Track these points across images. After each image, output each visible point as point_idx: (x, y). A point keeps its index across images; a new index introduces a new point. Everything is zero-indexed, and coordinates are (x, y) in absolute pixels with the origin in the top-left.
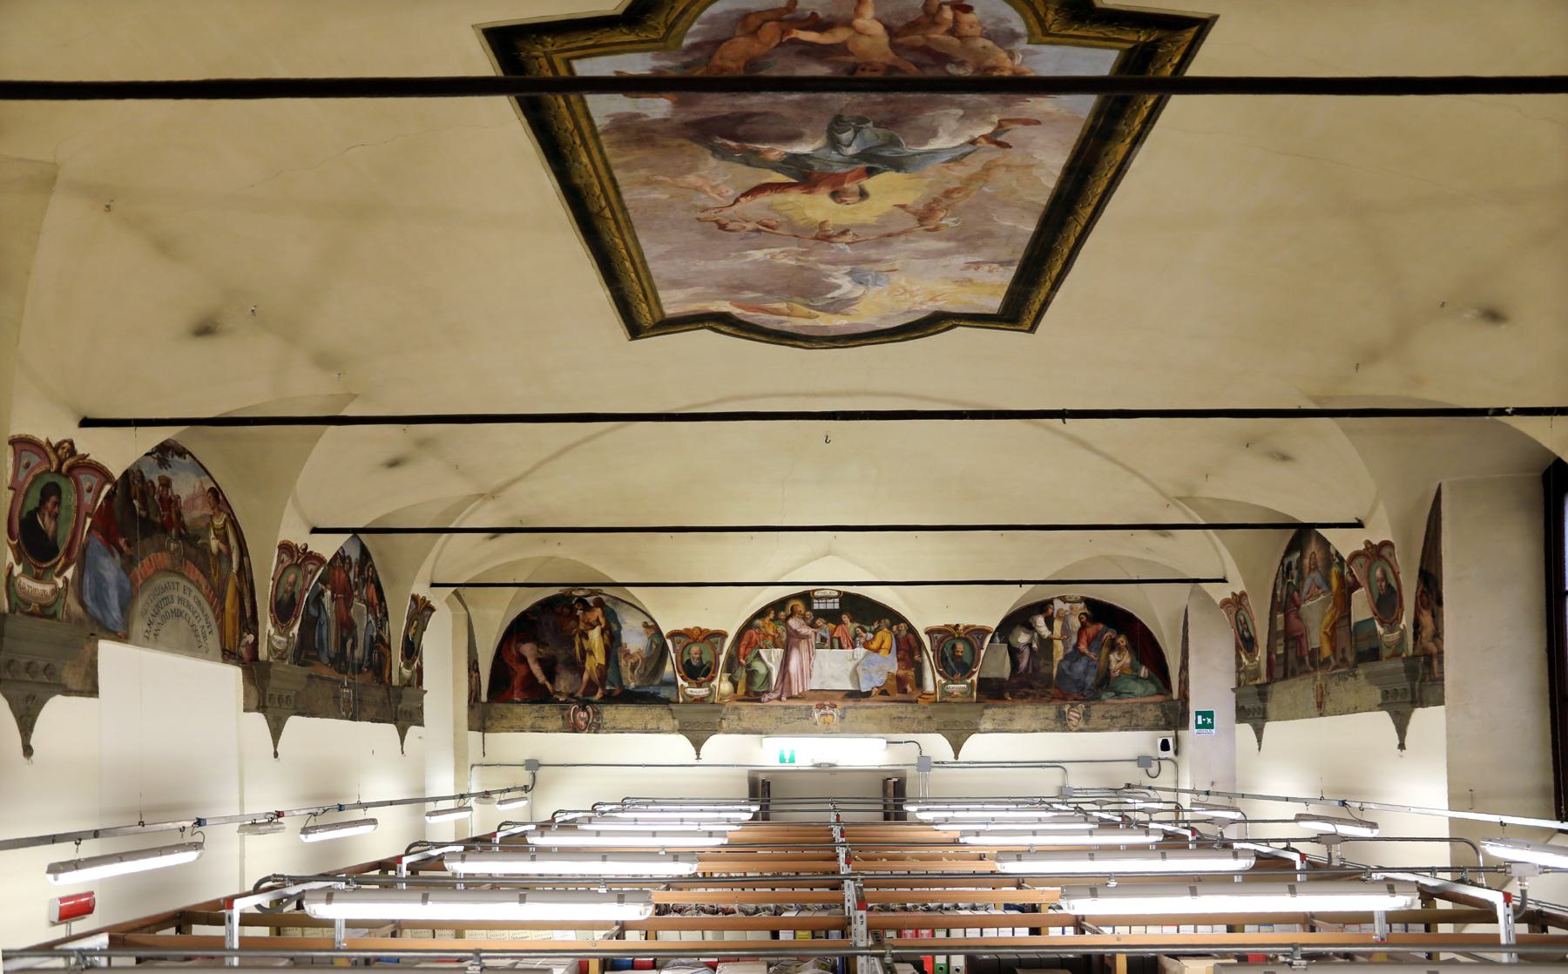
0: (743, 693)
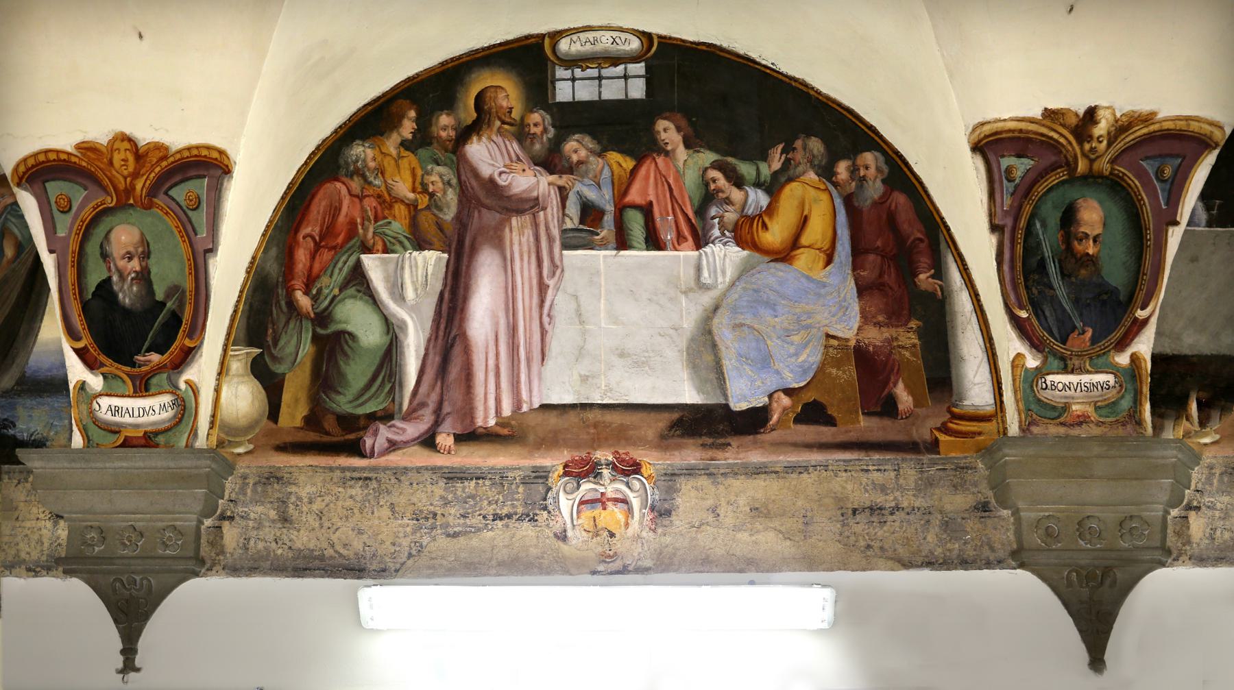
0: (298, 422)
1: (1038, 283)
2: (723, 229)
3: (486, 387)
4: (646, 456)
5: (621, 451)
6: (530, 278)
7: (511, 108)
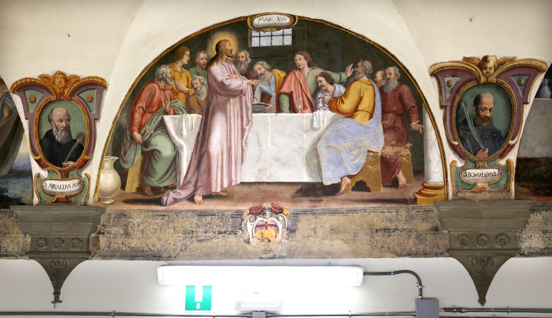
1: (463, 129)
2: (324, 103)
3: (217, 174)
4: (286, 205)
5: (275, 203)
6: (238, 126)
7: (232, 50)
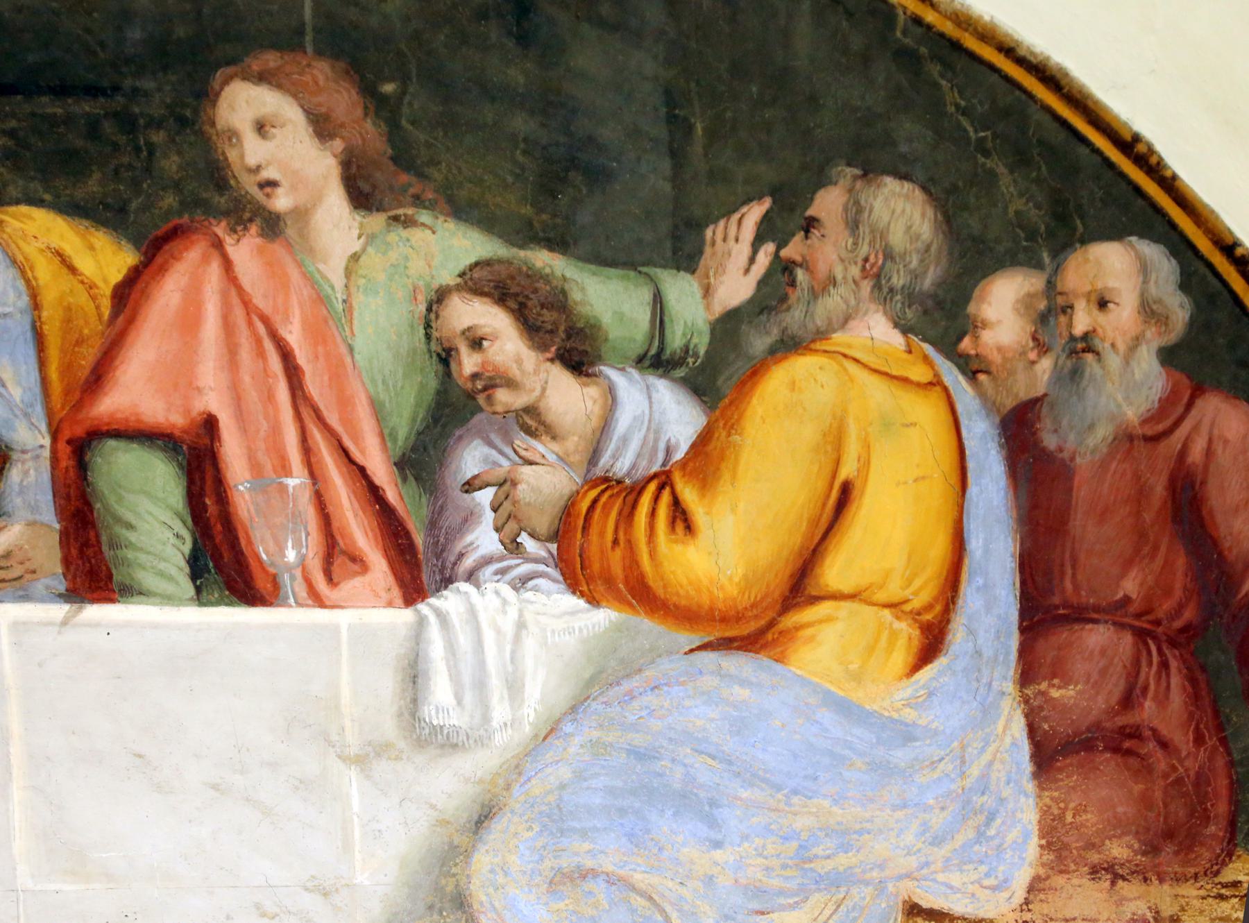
2: (512, 526)
